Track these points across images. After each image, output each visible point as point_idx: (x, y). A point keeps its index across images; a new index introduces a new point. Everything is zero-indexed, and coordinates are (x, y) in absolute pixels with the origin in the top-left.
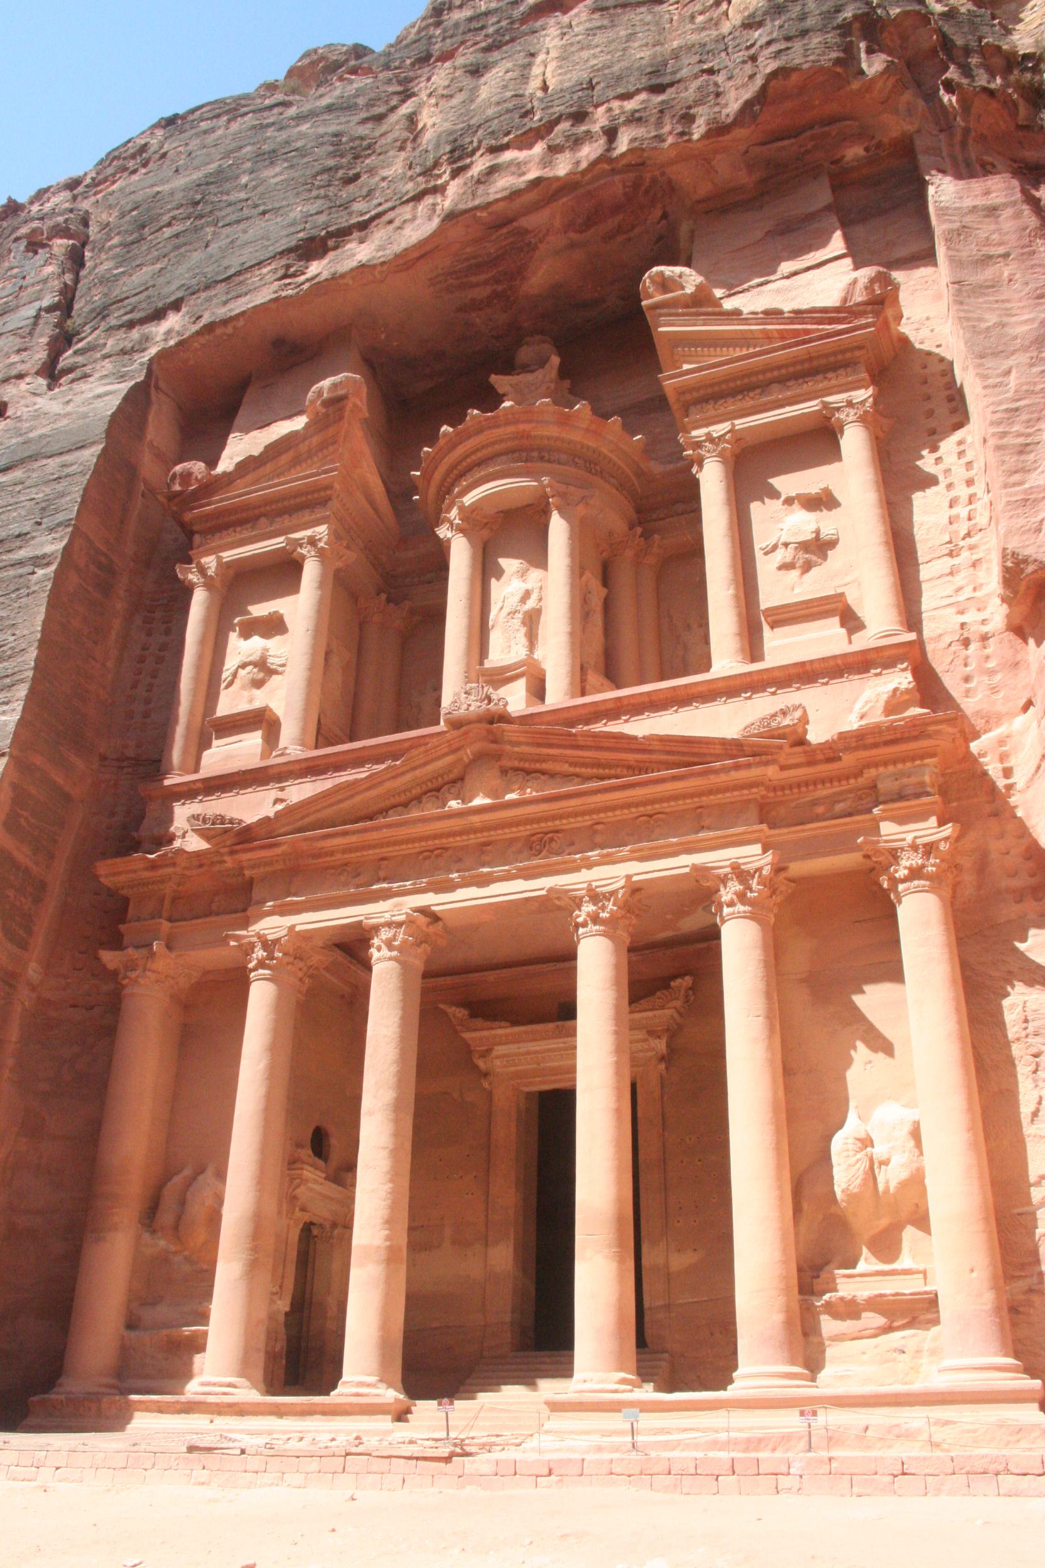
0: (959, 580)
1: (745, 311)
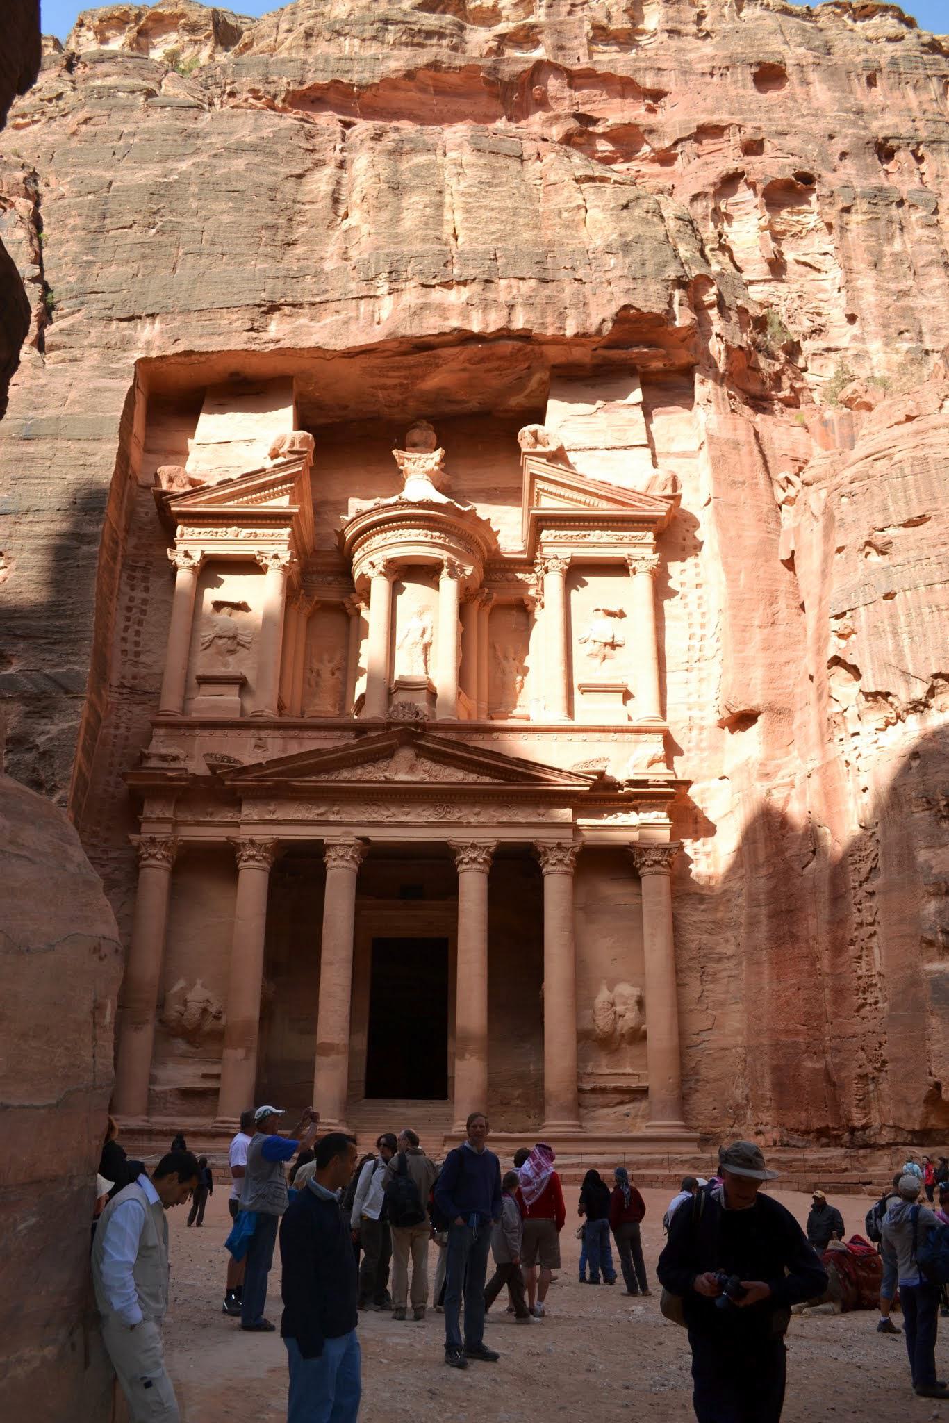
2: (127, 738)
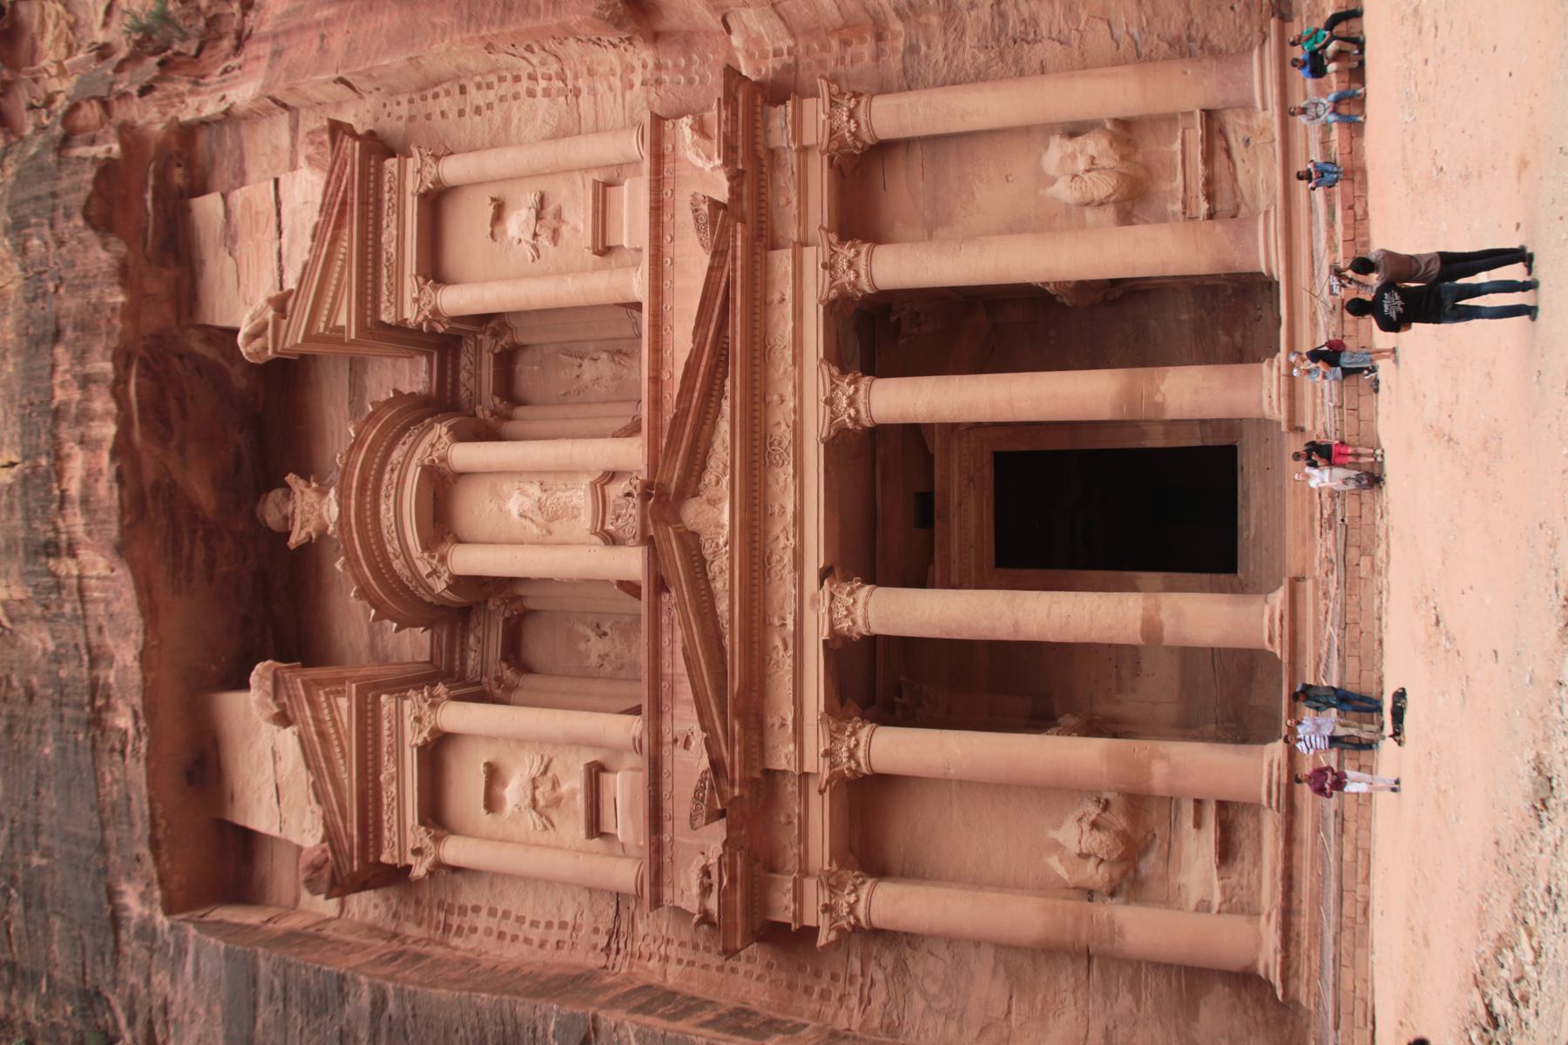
0: (602, 88)
1: (306, 257)
2: (682, 944)
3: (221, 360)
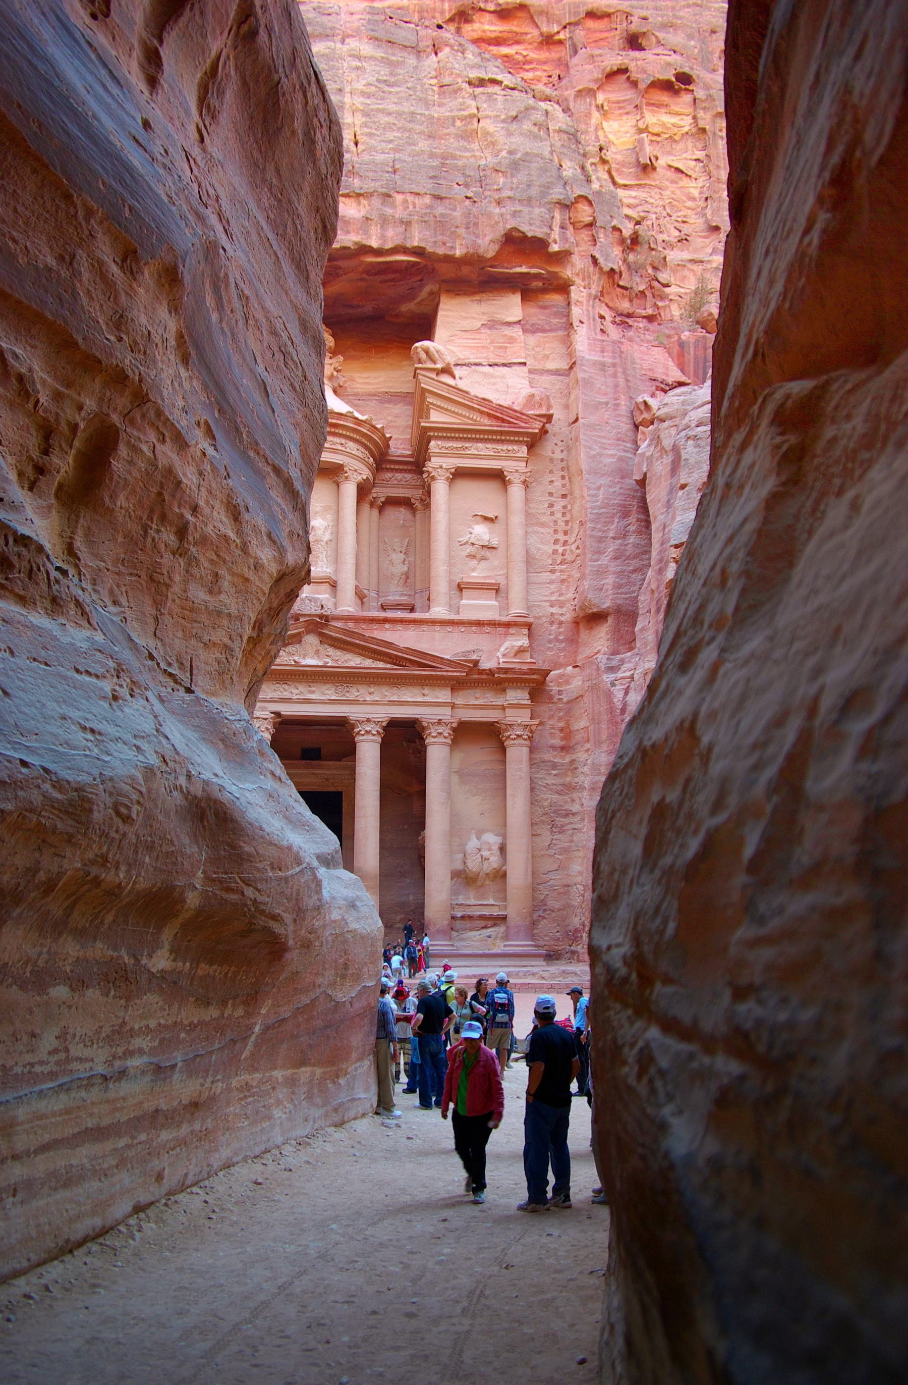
0: (553, 587)
3: (419, 299)
